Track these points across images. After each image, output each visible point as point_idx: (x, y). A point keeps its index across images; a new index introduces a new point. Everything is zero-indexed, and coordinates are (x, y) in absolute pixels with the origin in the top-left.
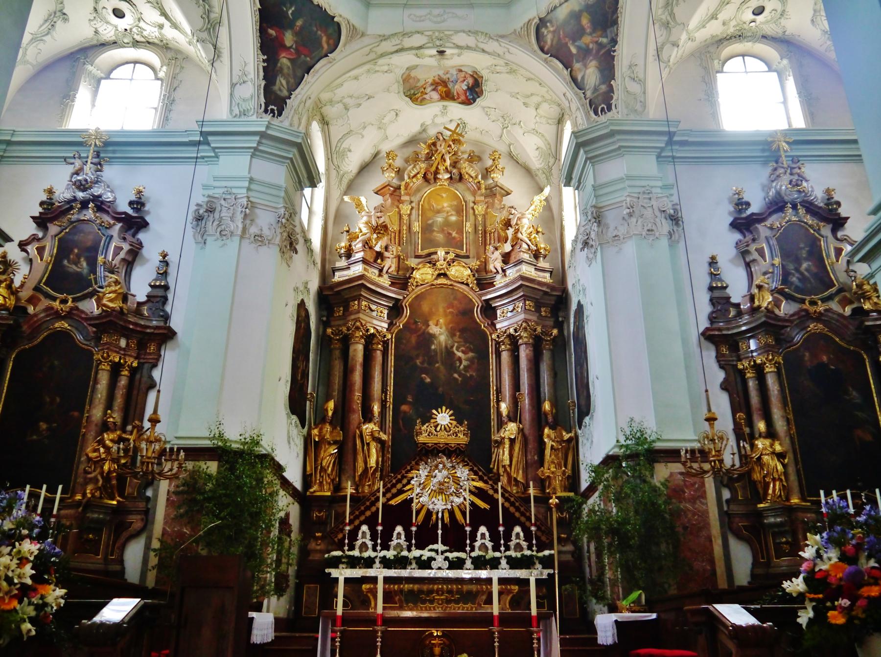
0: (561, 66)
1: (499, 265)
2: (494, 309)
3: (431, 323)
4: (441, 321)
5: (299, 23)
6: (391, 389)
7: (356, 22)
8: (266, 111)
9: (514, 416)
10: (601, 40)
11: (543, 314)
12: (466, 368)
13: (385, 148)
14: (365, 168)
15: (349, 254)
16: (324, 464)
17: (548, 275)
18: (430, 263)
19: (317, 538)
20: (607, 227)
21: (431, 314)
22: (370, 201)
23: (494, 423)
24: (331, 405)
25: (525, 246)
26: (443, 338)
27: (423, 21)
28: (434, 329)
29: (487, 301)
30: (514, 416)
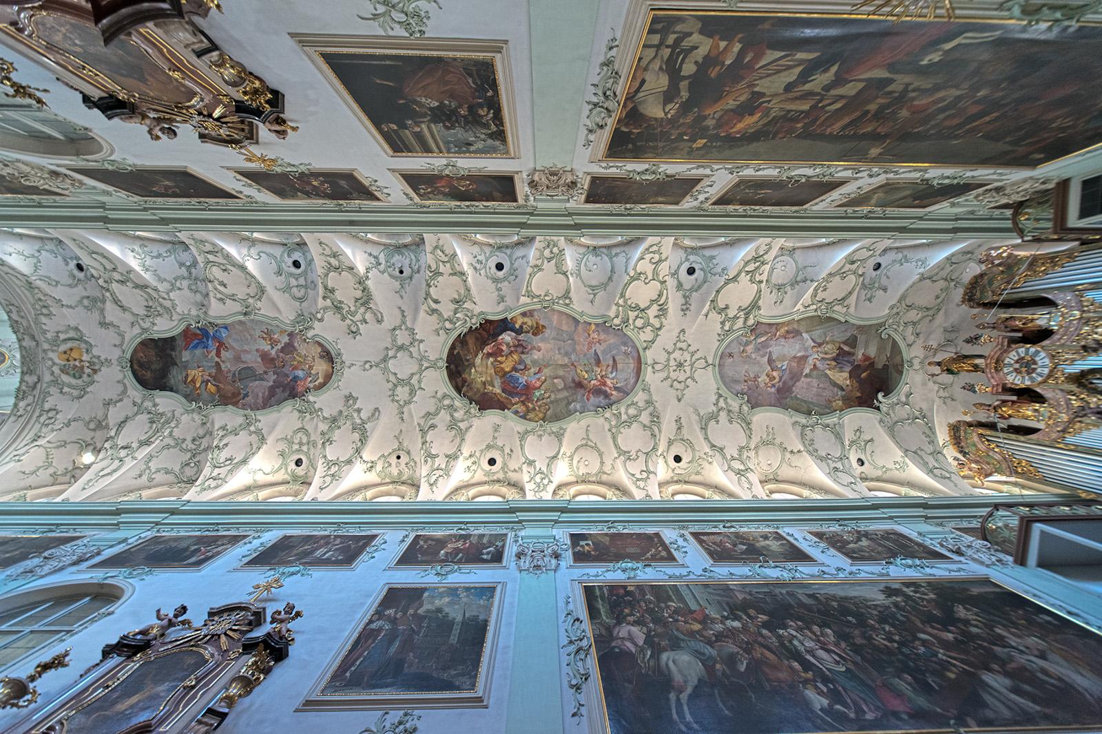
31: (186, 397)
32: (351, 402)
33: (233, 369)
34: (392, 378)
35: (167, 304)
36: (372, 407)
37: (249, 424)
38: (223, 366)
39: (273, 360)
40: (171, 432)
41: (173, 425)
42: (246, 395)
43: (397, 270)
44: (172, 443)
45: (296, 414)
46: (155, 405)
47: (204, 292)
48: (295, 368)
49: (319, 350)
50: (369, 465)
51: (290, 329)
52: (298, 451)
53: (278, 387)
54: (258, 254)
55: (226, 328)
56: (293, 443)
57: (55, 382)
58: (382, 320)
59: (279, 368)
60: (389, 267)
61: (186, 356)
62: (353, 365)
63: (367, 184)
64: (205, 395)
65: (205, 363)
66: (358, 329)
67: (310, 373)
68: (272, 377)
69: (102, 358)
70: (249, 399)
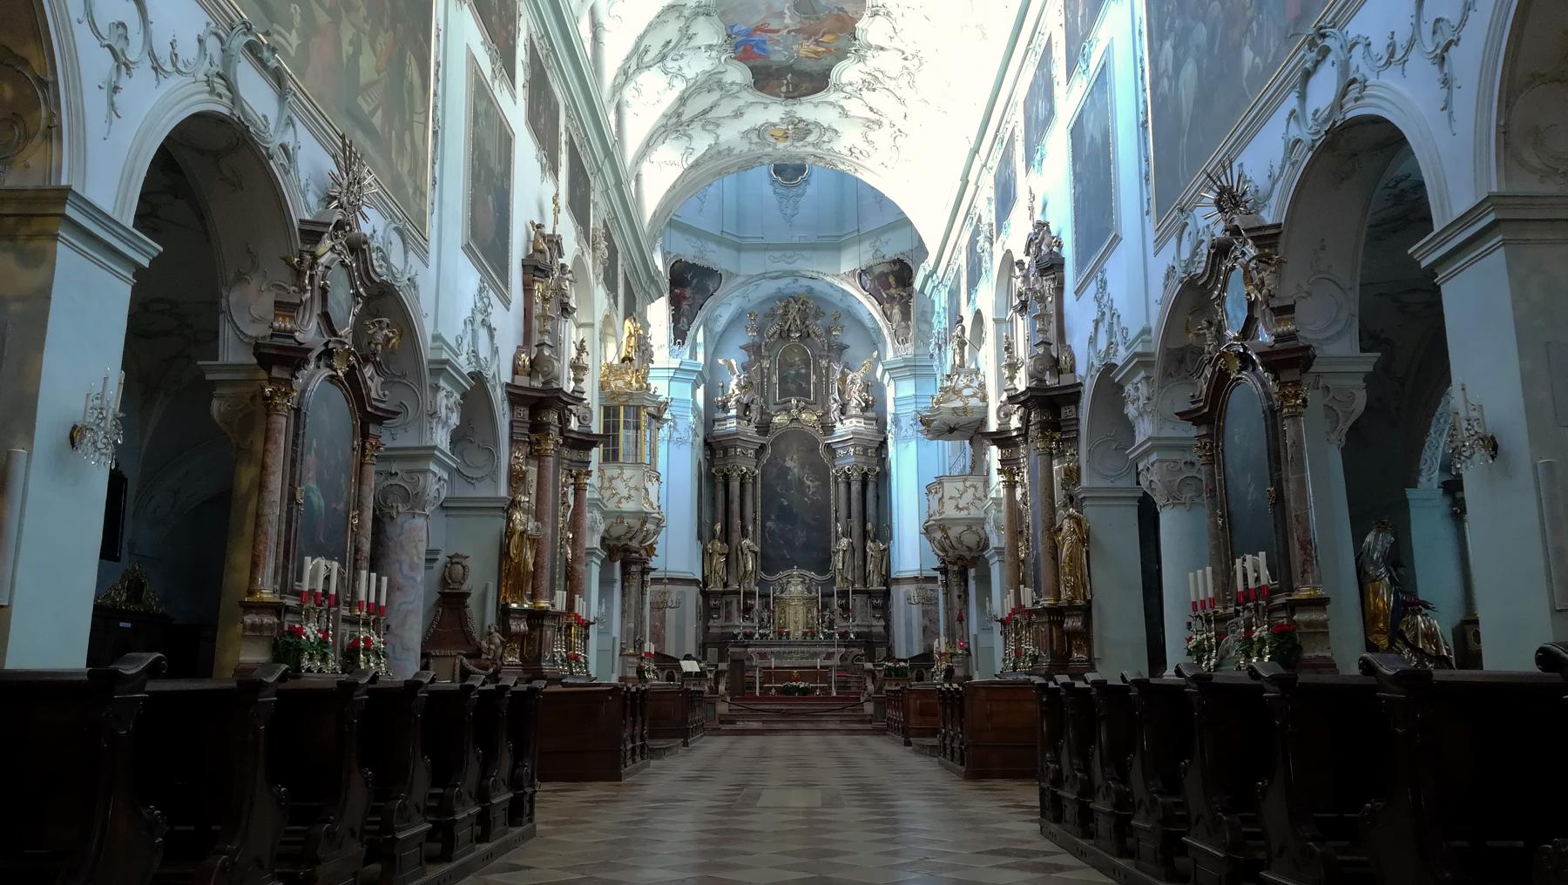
0: (877, 303)
2: (834, 450)
3: (787, 459)
4: (795, 457)
5: (695, 281)
6: (759, 509)
7: (732, 269)
8: (675, 344)
9: (847, 533)
10: (902, 293)
11: (869, 455)
14: (732, 323)
16: (717, 568)
17: (874, 422)
18: (785, 410)
19: (714, 619)
20: (901, 428)
23: (833, 539)
24: (718, 527)
25: (855, 401)
26: (796, 470)
27: (779, 262)
28: (789, 464)
29: (829, 444)
30: (847, 533)
31: (840, 59)
42: (842, 9)
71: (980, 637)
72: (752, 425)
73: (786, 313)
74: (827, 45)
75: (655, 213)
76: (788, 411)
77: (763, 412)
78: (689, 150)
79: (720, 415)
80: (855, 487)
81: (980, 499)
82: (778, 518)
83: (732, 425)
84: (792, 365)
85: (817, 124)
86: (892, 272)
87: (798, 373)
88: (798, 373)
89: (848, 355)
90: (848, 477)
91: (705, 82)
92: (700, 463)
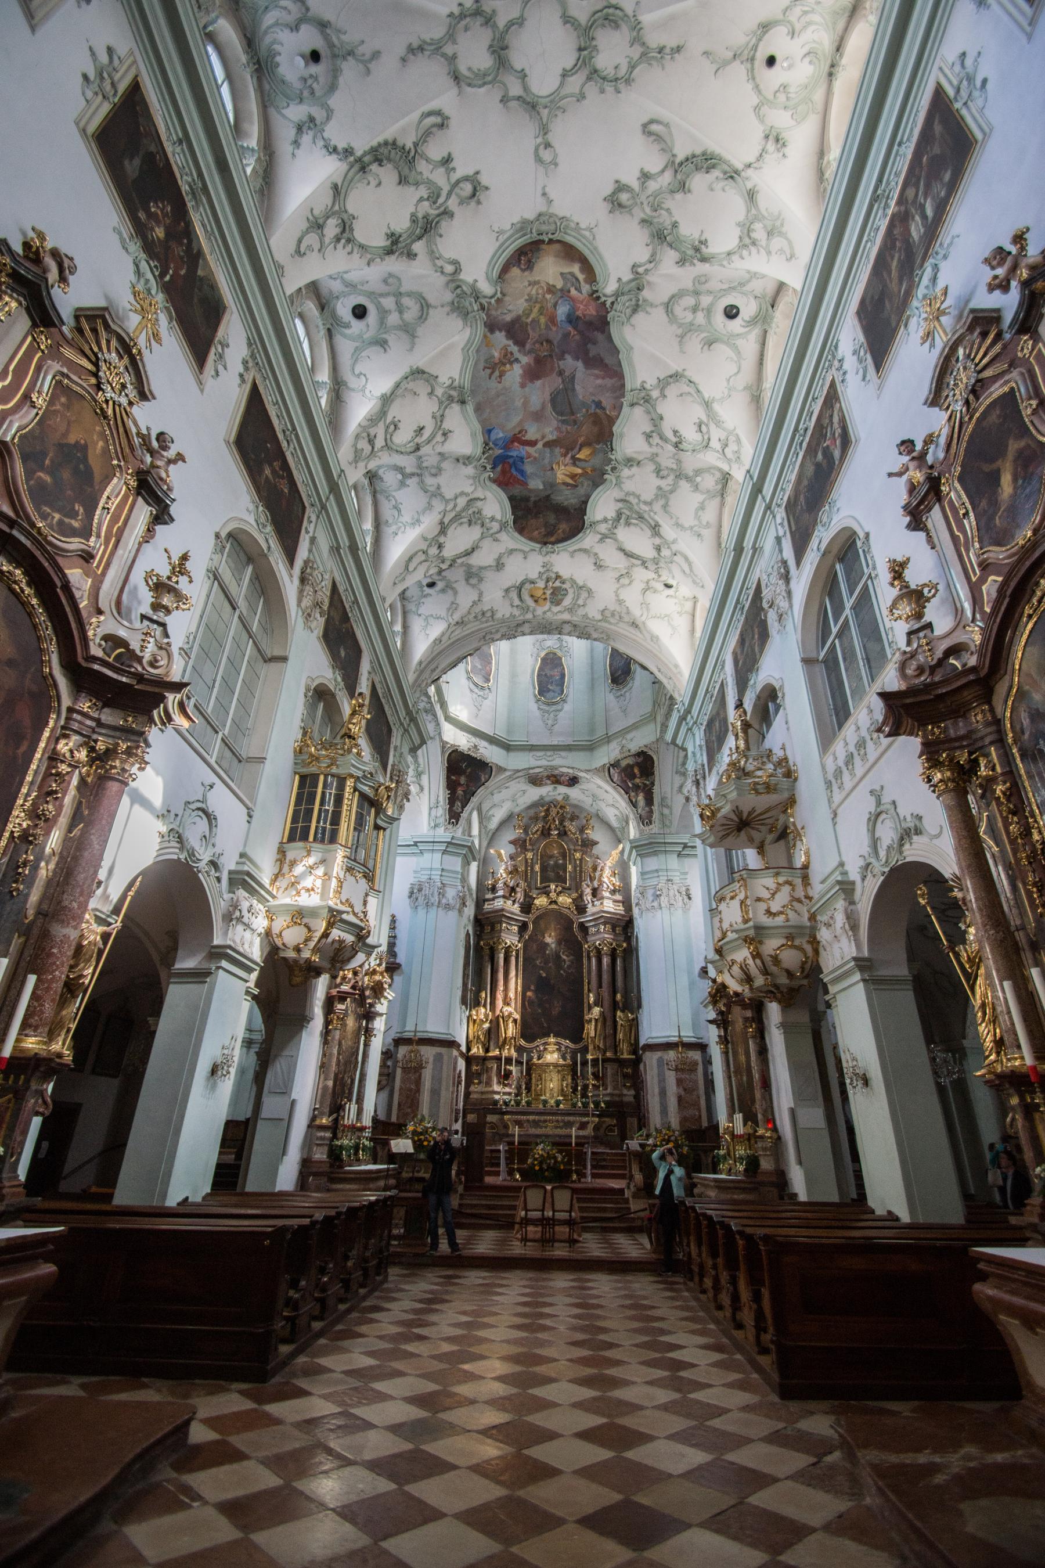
1: (589, 898)
12: (569, 967)
13: (517, 810)
14: (503, 824)
15: (494, 889)
21: (546, 929)
22: (505, 849)
28: (548, 940)
31: (596, 485)
32: (624, 197)
33: (555, 423)
34: (575, 82)
35: (462, 502)
36: (639, 140)
37: (647, 400)
38: (550, 437)
39: (538, 361)
40: (645, 503)
41: (634, 501)
42: (599, 404)
43: (314, 69)
44: (662, 502)
45: (639, 318)
46: (605, 520)
47: (438, 458)
48: (552, 319)
49: (515, 271)
50: (771, 146)
51: (481, 329)
52: (709, 311)
53: (587, 352)
54: (358, 376)
55: (489, 431)
56: (691, 324)
57: (570, 610)
58: (438, 113)
59: (552, 350)
60: (312, 93)
61: (536, 484)
62: (544, 194)
63: (106, 108)
64: (596, 461)
65: (546, 461)
66: (466, 179)
67: (562, 290)
68: (569, 363)
69: (542, 570)
70: (607, 401)
71: (801, 1113)
72: (516, 905)
73: (547, 816)
74: (583, 464)
75: (420, 663)
76: (547, 894)
77: (526, 895)
78: (453, 607)
79: (489, 896)
80: (606, 960)
81: (799, 901)
82: (535, 991)
83: (499, 904)
84: (551, 857)
85: (573, 581)
86: (637, 764)
87: (556, 863)
88: (556, 863)
89: (596, 850)
90: (599, 952)
91: (464, 510)
92: (468, 934)
